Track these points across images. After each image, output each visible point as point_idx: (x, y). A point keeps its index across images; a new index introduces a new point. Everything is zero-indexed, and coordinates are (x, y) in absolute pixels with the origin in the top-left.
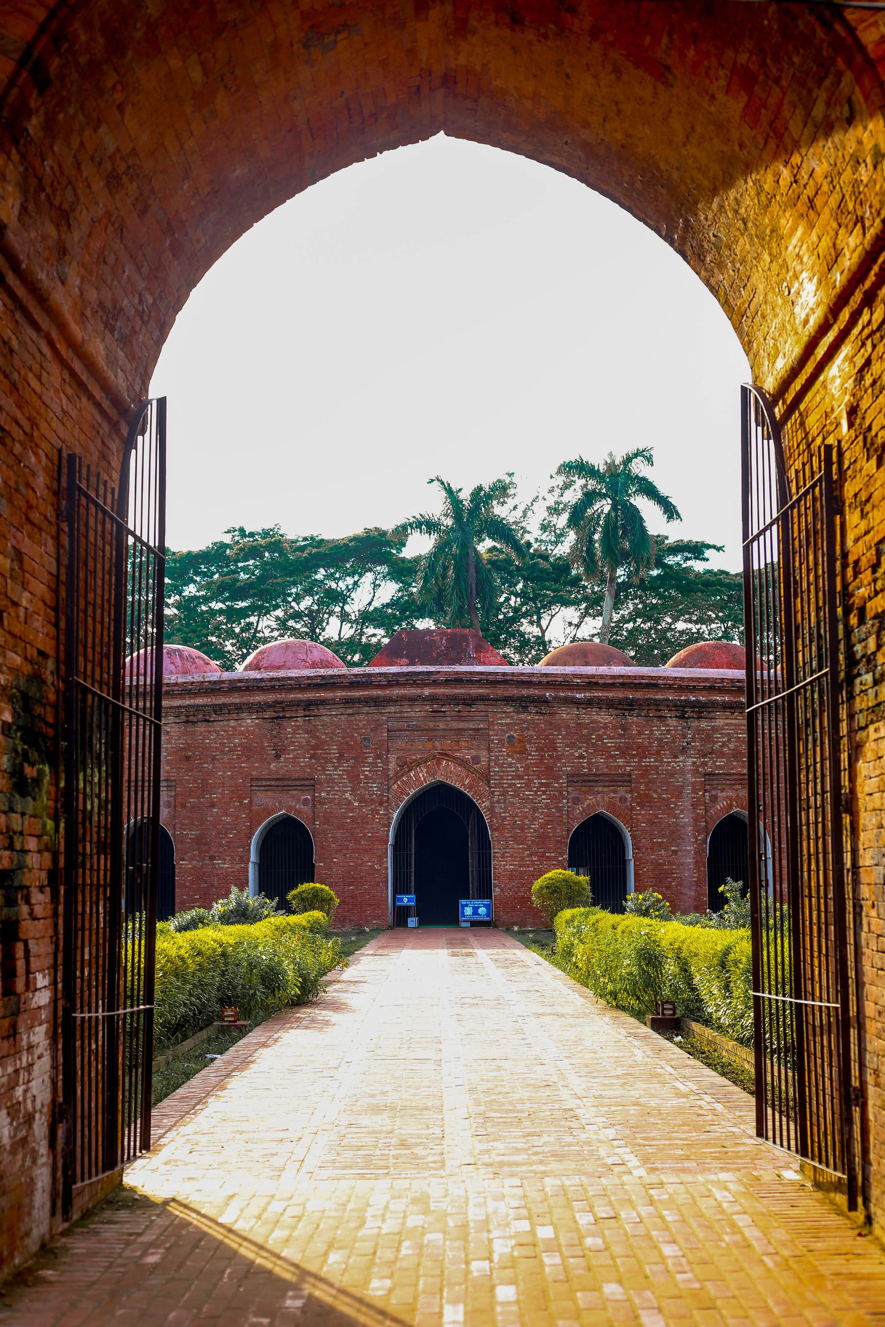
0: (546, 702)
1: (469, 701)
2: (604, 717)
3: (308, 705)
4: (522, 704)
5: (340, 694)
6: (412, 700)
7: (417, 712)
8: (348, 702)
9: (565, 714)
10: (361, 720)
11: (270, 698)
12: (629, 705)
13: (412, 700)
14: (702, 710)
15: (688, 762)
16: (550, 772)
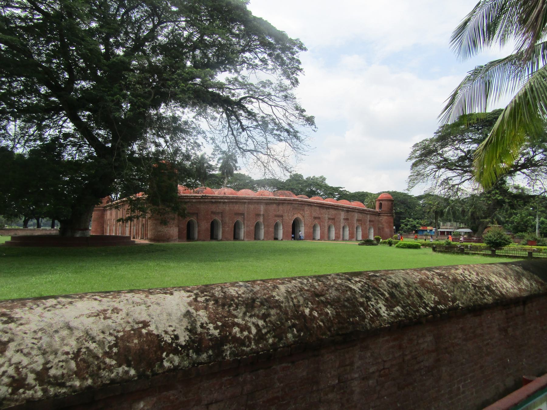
0: (311, 205)
1: (303, 204)
2: (318, 208)
3: (283, 203)
4: (309, 205)
5: (286, 202)
6: (296, 204)
7: (296, 206)
8: (288, 203)
9: (313, 208)
10: (289, 206)
11: (277, 202)
13: (296, 204)
14: (328, 208)
15: (327, 216)
16: (311, 216)
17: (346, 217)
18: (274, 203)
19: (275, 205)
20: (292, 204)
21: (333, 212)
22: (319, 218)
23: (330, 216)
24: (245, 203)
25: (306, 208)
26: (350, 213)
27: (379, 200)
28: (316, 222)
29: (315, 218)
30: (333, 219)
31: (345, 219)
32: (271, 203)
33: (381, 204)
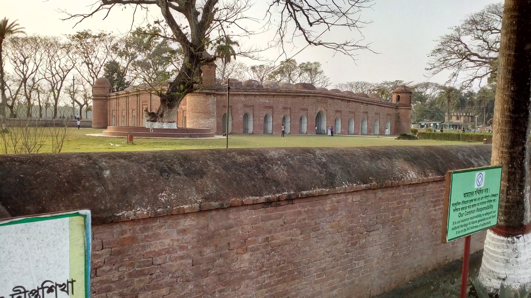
2: (340, 101)
9: (336, 101)
12: (342, 100)
17: (365, 111)
18: (300, 96)
19: (301, 98)
20: (316, 96)
21: (354, 105)
22: (341, 112)
23: (350, 110)
24: (274, 95)
25: (330, 101)
26: (369, 106)
27: (397, 93)
28: (338, 114)
29: (337, 111)
30: (353, 113)
31: (364, 112)
32: (297, 96)
33: (399, 96)
